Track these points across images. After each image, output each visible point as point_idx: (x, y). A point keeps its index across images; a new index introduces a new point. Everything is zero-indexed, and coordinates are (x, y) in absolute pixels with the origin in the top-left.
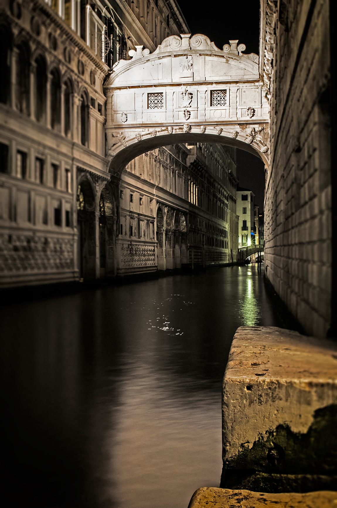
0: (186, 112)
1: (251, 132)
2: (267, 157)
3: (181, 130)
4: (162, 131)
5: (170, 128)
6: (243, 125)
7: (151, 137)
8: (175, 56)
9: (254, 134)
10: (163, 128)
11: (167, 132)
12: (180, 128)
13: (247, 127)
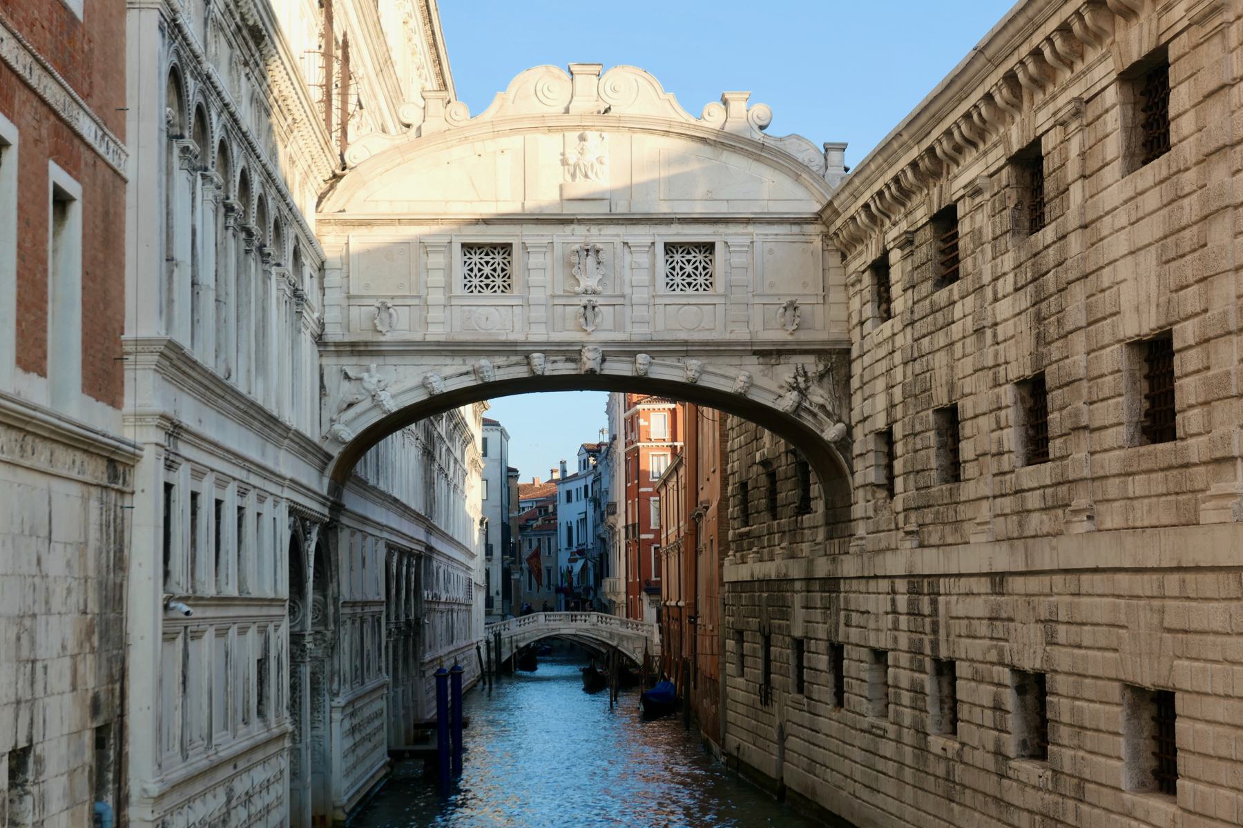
0: (589, 308)
1: (795, 378)
2: (844, 457)
3: (572, 365)
4: (509, 366)
5: (537, 359)
6: (771, 354)
7: (474, 383)
8: (550, 129)
9: (802, 385)
10: (514, 359)
11: (525, 368)
12: (568, 360)
13: (782, 362)
